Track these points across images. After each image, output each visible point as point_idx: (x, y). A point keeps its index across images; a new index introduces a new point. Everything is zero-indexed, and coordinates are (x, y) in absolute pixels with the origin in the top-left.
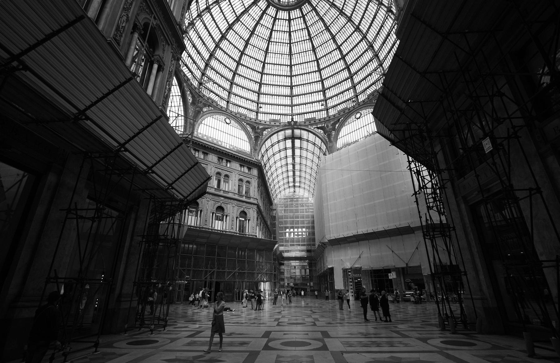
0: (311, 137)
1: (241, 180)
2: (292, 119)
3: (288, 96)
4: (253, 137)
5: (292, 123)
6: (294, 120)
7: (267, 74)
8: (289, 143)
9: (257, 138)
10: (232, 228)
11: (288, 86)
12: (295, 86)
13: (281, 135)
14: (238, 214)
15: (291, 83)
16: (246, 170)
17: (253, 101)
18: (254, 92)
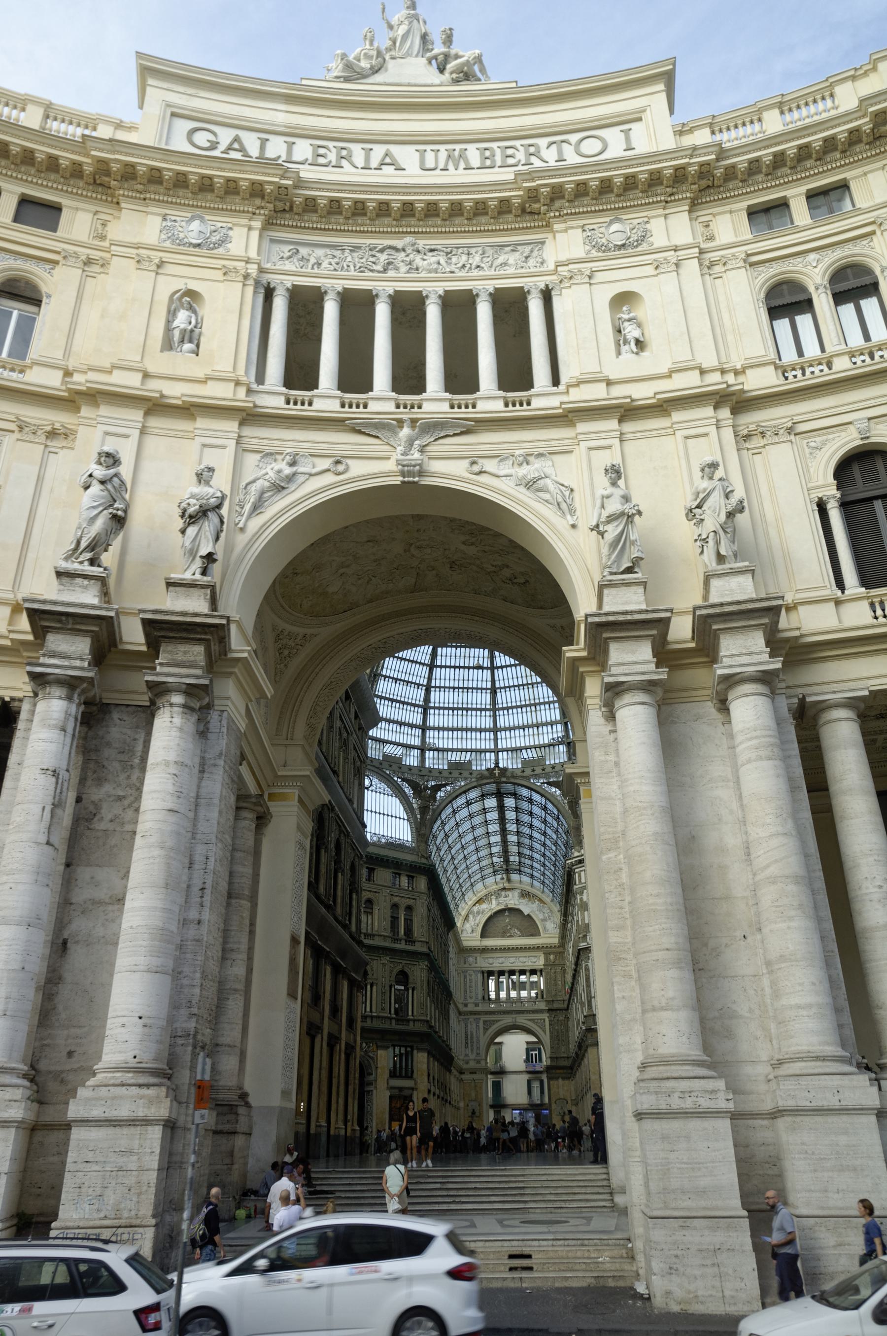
0: (536, 797)
1: (395, 906)
2: (497, 763)
3: (486, 710)
4: (415, 806)
5: (497, 772)
6: (501, 765)
7: (441, 667)
8: (491, 802)
9: (424, 810)
10: (383, 1009)
11: (486, 689)
12: (500, 688)
13: (473, 795)
14: (393, 979)
15: (493, 681)
16: (404, 881)
17: (412, 726)
18: (415, 705)
